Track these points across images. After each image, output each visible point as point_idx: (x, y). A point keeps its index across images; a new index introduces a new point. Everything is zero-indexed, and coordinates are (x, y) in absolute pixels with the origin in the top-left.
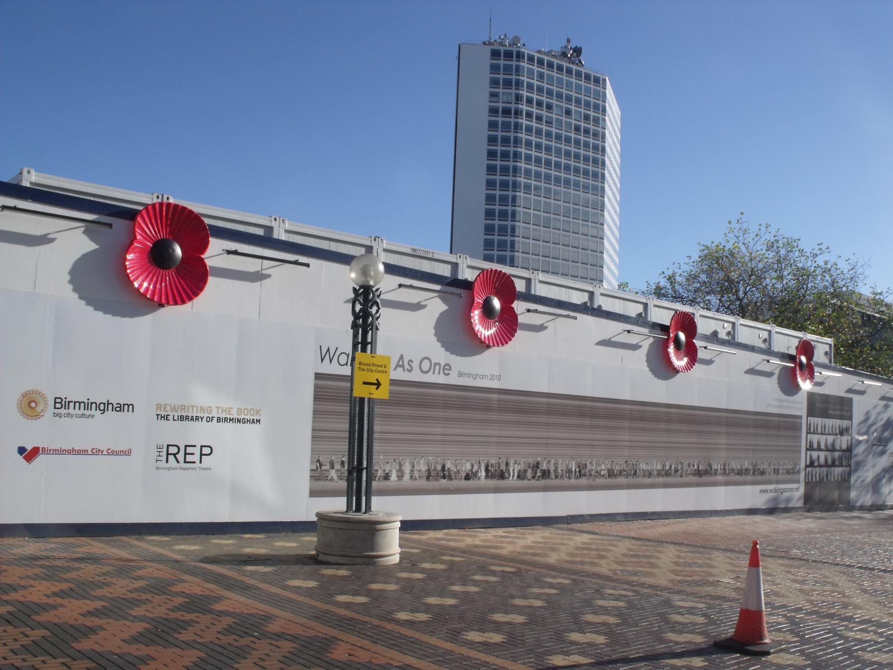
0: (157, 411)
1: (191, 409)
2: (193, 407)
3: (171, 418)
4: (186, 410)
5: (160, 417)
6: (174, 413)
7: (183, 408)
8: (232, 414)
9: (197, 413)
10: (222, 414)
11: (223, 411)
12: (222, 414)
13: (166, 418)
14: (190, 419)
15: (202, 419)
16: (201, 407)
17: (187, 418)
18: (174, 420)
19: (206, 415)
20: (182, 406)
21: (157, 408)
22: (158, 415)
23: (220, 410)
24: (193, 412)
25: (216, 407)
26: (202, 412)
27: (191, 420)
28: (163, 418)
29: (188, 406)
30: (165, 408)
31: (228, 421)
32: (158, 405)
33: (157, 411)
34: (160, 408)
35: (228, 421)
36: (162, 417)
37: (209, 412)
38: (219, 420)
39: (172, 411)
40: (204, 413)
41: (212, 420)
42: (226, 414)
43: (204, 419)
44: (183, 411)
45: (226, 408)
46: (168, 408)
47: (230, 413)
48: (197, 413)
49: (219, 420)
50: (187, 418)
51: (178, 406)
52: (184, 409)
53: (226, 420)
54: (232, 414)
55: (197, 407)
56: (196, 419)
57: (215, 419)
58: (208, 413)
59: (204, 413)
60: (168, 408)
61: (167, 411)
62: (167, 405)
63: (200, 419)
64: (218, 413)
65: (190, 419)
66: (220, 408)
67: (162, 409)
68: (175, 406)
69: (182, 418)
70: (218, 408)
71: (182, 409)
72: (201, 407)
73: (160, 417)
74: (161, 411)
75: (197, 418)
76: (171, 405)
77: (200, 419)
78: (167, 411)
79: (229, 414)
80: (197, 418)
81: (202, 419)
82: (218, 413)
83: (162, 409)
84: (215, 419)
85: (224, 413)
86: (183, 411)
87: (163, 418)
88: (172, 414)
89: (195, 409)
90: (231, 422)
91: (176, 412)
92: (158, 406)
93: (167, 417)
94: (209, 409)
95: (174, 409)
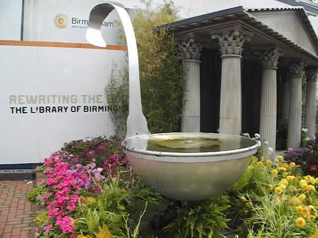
0: (11, 103)
1: (51, 99)
2: (54, 96)
3: (28, 110)
4: (46, 100)
5: (15, 110)
6: (31, 105)
7: (42, 98)
8: (101, 102)
9: (60, 102)
10: (89, 102)
11: (90, 99)
12: (89, 102)
13: (22, 110)
14: (51, 110)
15: (66, 109)
16: (64, 97)
17: (48, 109)
18: (32, 112)
19: (70, 105)
20: (40, 96)
21: (11, 100)
22: (12, 108)
23: (87, 98)
24: (54, 103)
25: (82, 96)
26: (65, 102)
27: (53, 111)
28: (18, 112)
29: (48, 96)
30: (20, 100)
31: (97, 109)
32: (11, 96)
33: (11, 103)
34: (14, 100)
35: (97, 109)
36: (17, 110)
37: (74, 101)
38: (86, 109)
39: (29, 103)
40: (68, 103)
41: (78, 109)
42: (94, 102)
43: (69, 110)
44: (42, 102)
45: (94, 96)
46: (24, 100)
47: (99, 100)
48: (60, 102)
49: (86, 109)
50: (48, 109)
51: (36, 96)
52: (44, 100)
53: (94, 108)
54: (101, 102)
55: (59, 96)
56: (59, 110)
57: (82, 109)
58: (72, 102)
59: (68, 103)
60: (24, 100)
61: (24, 103)
62: (23, 96)
63: (63, 110)
64: (84, 102)
65: (51, 110)
66: (86, 96)
67: (17, 101)
68: (32, 96)
69: (42, 110)
70: (84, 96)
71: (40, 99)
72: (64, 97)
73: (15, 110)
74: (15, 103)
75: (60, 109)
76: (27, 96)
77: (63, 110)
78: (24, 103)
79: (98, 102)
80: (60, 109)
81: (66, 109)
82: (84, 102)
83: (17, 101)
84: (82, 109)
85: (92, 101)
86: (42, 102)
87: (18, 112)
88: (29, 106)
89: (57, 99)
90: (101, 111)
91: (34, 103)
92: (12, 98)
93: (23, 110)
94: (74, 98)
95: (32, 100)
